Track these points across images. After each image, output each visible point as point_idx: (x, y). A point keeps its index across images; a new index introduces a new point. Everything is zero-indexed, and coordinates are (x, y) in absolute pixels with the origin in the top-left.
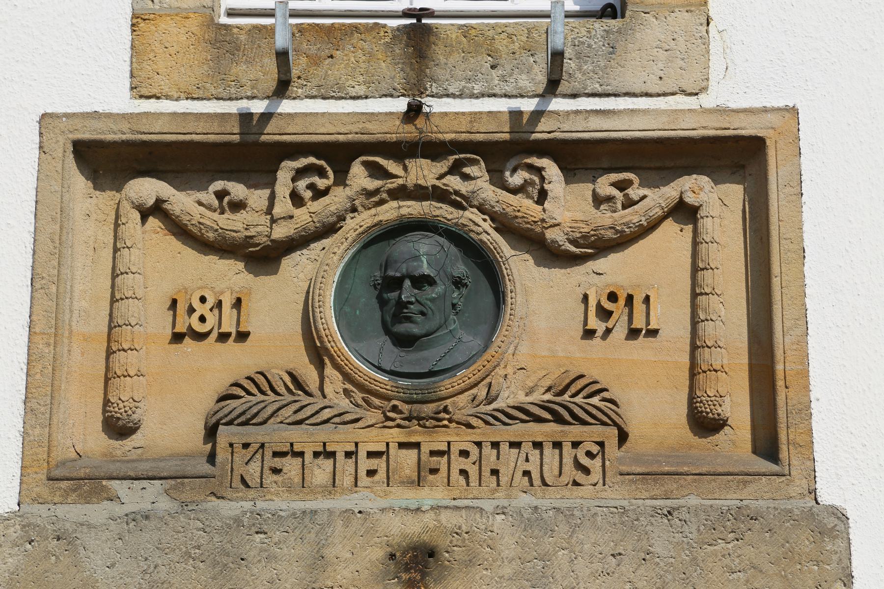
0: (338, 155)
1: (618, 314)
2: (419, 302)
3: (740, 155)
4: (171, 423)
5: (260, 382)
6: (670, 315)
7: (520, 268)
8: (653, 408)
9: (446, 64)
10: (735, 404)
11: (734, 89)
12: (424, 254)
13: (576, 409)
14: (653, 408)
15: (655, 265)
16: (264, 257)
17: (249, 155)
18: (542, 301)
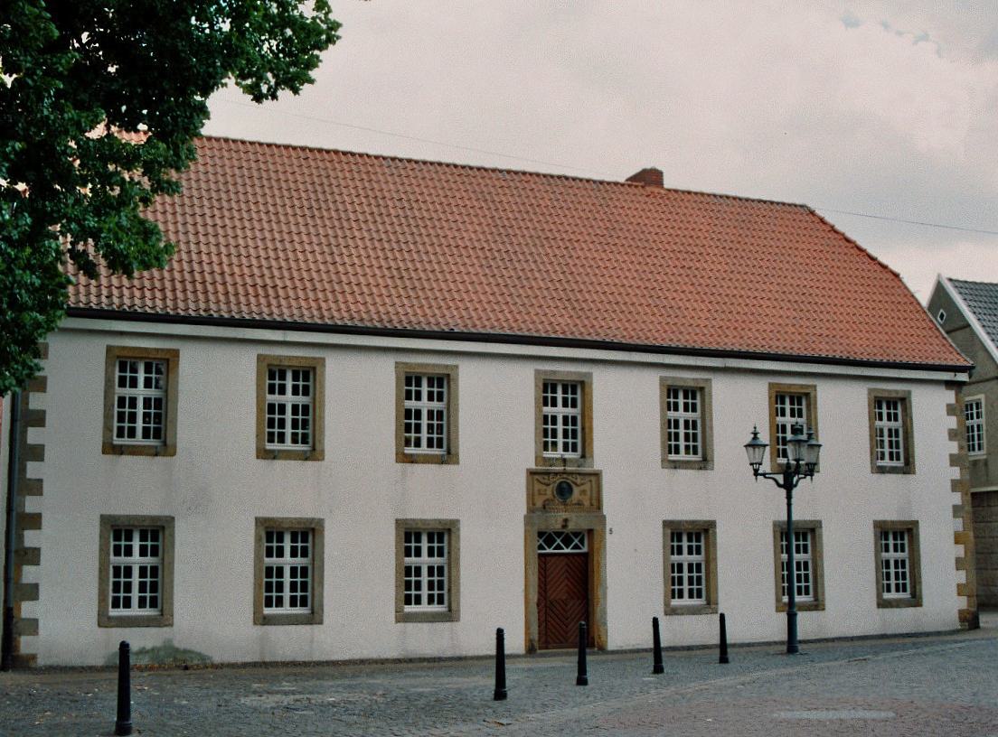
0: (556, 474)
1: (583, 492)
2: (564, 491)
3: (597, 475)
4: (539, 504)
5: (548, 500)
6: (589, 493)
7: (574, 486)
8: (587, 503)
9: (568, 463)
10: (594, 502)
11: (597, 467)
12: (565, 485)
13: (579, 504)
14: (587, 503)
15: (587, 487)
16: (548, 485)
17: (547, 473)
18: (576, 490)
